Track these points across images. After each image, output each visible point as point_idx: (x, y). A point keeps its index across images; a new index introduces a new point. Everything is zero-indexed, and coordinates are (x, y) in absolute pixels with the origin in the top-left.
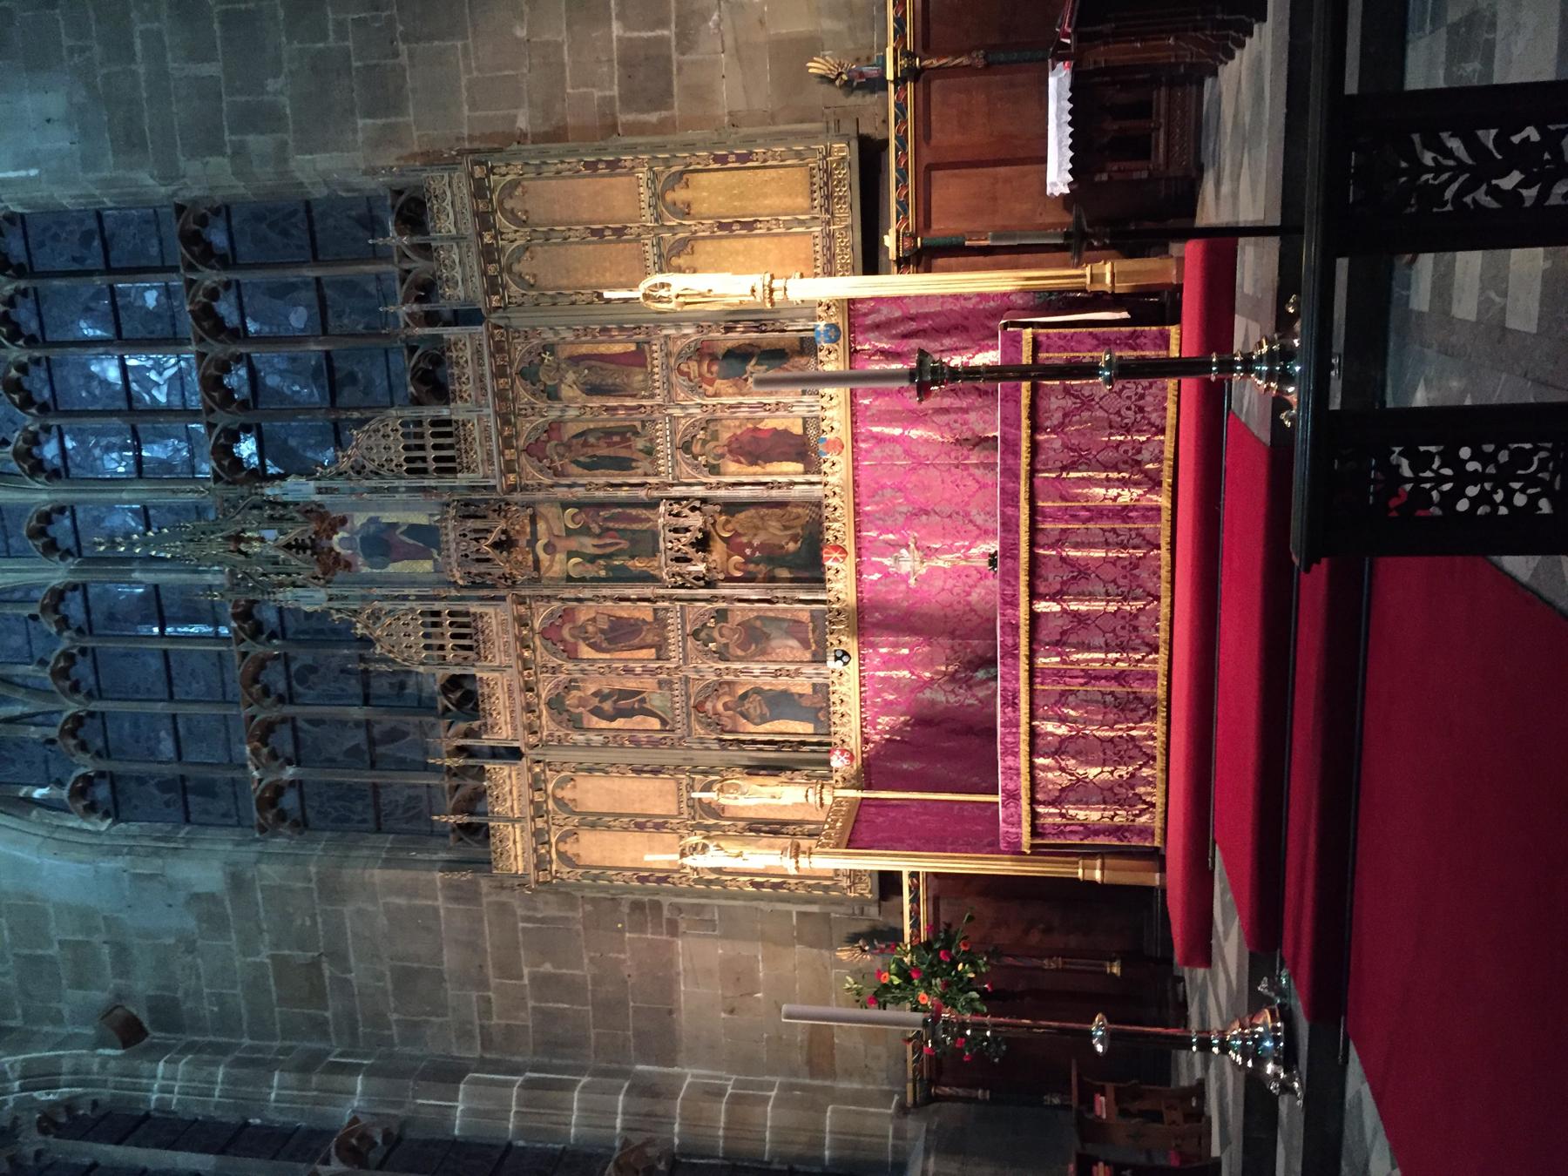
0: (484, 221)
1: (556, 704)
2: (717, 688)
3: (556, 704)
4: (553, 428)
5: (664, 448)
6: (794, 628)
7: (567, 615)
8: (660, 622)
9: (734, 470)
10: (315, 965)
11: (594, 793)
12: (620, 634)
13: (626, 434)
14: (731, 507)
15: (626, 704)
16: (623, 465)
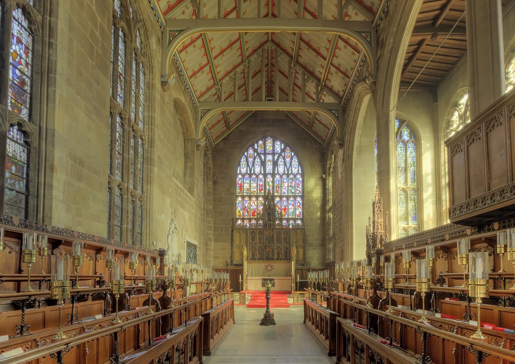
0: (300, 229)
1: (253, 232)
2: (256, 249)
3: (253, 232)
4: (280, 234)
5: (278, 245)
6: (261, 257)
7: (262, 234)
8: (261, 243)
9: (276, 251)
10: (223, 202)
11: (243, 235)
12: (260, 239)
13: (280, 241)
14: (273, 251)
15: (253, 239)
16: (277, 240)
